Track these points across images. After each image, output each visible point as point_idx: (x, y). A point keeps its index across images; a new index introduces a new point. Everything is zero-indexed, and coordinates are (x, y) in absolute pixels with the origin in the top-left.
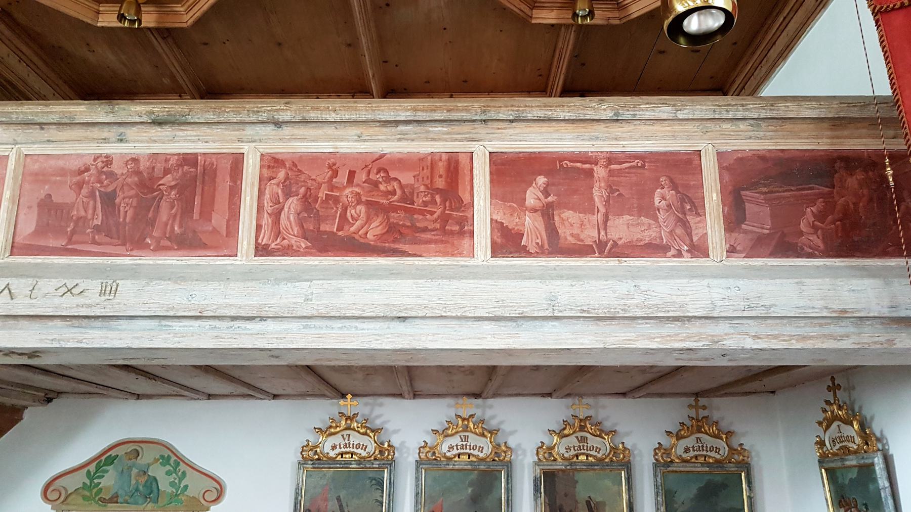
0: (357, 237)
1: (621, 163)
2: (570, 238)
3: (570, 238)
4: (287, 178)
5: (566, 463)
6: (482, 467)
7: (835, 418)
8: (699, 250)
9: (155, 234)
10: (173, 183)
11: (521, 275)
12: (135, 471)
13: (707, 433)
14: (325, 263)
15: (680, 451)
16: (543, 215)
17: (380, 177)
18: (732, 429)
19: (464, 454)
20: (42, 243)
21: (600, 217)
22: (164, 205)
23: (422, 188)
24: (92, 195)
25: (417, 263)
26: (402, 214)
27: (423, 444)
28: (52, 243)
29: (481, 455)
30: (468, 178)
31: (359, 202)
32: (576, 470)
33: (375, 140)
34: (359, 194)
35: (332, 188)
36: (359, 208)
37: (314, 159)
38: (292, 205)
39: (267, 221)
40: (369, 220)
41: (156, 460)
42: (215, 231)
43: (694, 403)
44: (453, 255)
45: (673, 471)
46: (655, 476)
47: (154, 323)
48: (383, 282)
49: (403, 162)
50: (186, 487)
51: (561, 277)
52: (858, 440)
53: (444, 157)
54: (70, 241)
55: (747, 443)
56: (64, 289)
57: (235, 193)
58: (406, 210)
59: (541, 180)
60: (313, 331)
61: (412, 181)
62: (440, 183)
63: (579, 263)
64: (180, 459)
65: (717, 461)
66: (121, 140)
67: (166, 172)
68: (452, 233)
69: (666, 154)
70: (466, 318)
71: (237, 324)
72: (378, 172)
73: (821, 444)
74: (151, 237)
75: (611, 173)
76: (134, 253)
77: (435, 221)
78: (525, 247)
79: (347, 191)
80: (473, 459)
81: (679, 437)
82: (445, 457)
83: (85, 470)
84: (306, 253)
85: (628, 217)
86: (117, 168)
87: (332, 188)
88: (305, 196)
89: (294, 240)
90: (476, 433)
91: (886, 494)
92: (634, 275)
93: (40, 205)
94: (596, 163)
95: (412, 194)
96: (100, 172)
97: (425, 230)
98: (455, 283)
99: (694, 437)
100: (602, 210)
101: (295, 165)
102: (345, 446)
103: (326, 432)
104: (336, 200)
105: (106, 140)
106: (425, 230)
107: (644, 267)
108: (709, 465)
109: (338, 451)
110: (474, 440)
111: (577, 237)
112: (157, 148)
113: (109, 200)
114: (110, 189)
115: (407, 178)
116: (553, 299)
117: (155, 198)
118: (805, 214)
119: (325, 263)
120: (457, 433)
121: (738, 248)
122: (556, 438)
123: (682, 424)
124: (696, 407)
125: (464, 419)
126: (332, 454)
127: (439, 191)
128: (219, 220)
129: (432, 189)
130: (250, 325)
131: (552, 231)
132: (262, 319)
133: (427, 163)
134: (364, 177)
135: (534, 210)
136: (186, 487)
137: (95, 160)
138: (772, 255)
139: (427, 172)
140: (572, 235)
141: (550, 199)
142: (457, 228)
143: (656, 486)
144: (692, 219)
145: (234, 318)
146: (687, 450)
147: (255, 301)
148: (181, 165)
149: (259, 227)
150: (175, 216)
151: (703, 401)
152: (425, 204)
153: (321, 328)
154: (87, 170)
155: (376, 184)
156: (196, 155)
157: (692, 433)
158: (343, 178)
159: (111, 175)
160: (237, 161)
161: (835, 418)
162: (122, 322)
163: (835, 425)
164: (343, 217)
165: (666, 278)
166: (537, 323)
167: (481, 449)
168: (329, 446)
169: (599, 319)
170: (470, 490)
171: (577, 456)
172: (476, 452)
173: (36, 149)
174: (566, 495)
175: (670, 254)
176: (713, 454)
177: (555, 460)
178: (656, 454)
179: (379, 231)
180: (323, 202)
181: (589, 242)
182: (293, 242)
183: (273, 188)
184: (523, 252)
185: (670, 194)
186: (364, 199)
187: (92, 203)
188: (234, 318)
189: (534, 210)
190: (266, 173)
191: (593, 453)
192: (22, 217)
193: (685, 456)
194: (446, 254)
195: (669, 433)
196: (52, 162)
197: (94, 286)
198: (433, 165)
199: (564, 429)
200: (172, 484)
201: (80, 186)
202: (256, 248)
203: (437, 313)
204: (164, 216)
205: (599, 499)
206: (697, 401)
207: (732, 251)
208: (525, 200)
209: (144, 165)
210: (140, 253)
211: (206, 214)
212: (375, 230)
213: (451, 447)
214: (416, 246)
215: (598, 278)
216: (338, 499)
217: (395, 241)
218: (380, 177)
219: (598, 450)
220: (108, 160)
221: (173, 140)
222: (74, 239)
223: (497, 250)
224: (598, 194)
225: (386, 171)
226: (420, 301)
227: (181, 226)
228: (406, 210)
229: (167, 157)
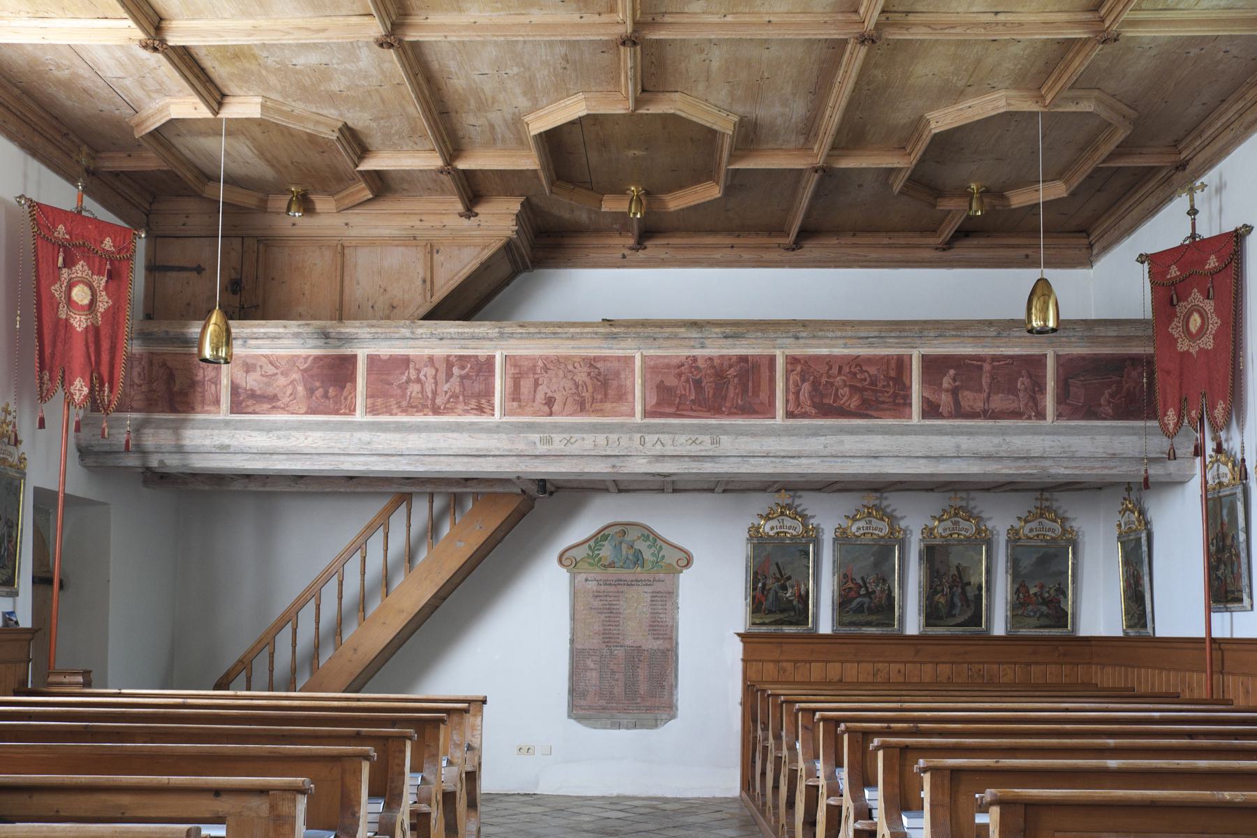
0: (844, 407)
1: (999, 361)
2: (967, 408)
3: (967, 408)
4: (802, 370)
5: (942, 539)
6: (881, 543)
7: (1127, 509)
8: (1041, 415)
9: (728, 404)
10: (735, 374)
11: (940, 432)
12: (624, 546)
13: (1047, 518)
14: (828, 423)
15: (1026, 531)
16: (952, 394)
17: (856, 370)
18: (1067, 515)
19: (868, 533)
20: (662, 410)
21: (985, 395)
22: (731, 388)
23: (882, 377)
24: (687, 381)
25: (880, 423)
26: (870, 393)
27: (837, 526)
28: (667, 410)
29: (881, 534)
30: (909, 371)
31: (845, 386)
32: (950, 545)
33: (854, 347)
34: (844, 381)
35: (829, 377)
36: (845, 389)
37: (817, 358)
38: (806, 387)
39: (791, 397)
40: (851, 397)
41: (639, 538)
42: (762, 403)
43: (1039, 497)
44: (900, 418)
45: (1020, 546)
46: (1007, 548)
47: (740, 459)
48: (866, 437)
49: (870, 360)
50: (663, 557)
51: (962, 433)
52: (1136, 523)
53: (895, 357)
54: (678, 409)
55: (1075, 525)
56: (690, 441)
57: (772, 380)
58: (872, 390)
59: (952, 372)
60: (827, 464)
61: (876, 372)
62: (893, 374)
63: (972, 423)
64: (657, 537)
65: (1053, 539)
66: (702, 347)
67: (731, 366)
68: (899, 405)
69: (1026, 355)
70: (911, 457)
71: (785, 460)
72: (856, 367)
73: (1120, 526)
74: (725, 407)
75: (994, 367)
76: (716, 416)
77: (889, 397)
78: (941, 413)
79: (838, 379)
80: (875, 537)
81: (1026, 521)
82: (854, 535)
83: (586, 545)
84: (816, 416)
85: (1001, 395)
86: (700, 364)
87: (829, 377)
88: (813, 382)
89: (808, 409)
90: (877, 518)
91: (1145, 556)
92: (1004, 432)
93: (657, 387)
94: (985, 361)
95: (876, 380)
96: (691, 367)
97: (883, 402)
98: (906, 438)
99: (1037, 521)
100: (987, 391)
101: (806, 362)
102: (781, 527)
103: (768, 518)
104: (832, 384)
105: (693, 347)
106: (883, 402)
107: (1008, 426)
108: (1047, 541)
109: (775, 531)
110: (876, 523)
111: (971, 407)
112: (725, 352)
113: (698, 384)
114: (698, 377)
115: (873, 370)
116: (958, 447)
117: (725, 383)
118: (1104, 393)
119: (828, 423)
120: (864, 518)
121: (1064, 414)
122: (936, 523)
123: (1030, 512)
124: (1041, 499)
125: (869, 508)
126: (772, 533)
127: (892, 378)
128: (764, 396)
129: (890, 379)
130: (792, 461)
131: (957, 403)
132: (799, 457)
133: (885, 360)
134: (848, 370)
135: (947, 391)
136: (663, 557)
137: (687, 359)
138: (1082, 419)
139: (884, 367)
140: (969, 406)
141: (957, 384)
142: (902, 401)
143: (1007, 556)
144: (1038, 396)
145: (784, 457)
146: (1031, 530)
147: (796, 448)
148: (738, 363)
149: (787, 401)
150: (738, 394)
151: (1046, 495)
152: (884, 386)
153: (831, 462)
154: (683, 365)
155: (855, 374)
156: (747, 356)
157: (1036, 518)
158: (835, 371)
159: (697, 368)
160: (772, 359)
161: (1127, 509)
162: (721, 458)
163: (1128, 512)
164: (836, 395)
165: (1020, 434)
166: (949, 459)
167: (881, 530)
168: (767, 528)
169: (983, 457)
170: (872, 559)
171: (951, 535)
172: (877, 532)
173: (652, 352)
174: (942, 562)
175: (1024, 417)
176: (1050, 533)
177: (935, 537)
178: (1009, 533)
179: (857, 403)
180: (824, 385)
181: (978, 410)
182: (808, 410)
183: (794, 377)
184: (939, 416)
185: (1027, 381)
186: (848, 383)
187: (688, 386)
188: (784, 457)
189: (947, 391)
190: (790, 367)
191: (963, 532)
192: (648, 394)
193: (1029, 535)
194: (895, 417)
195: (1019, 519)
196: (662, 360)
197: (707, 439)
198: (888, 362)
199: (943, 515)
200: (653, 554)
201: (680, 375)
202: (786, 413)
203: (896, 454)
204: (731, 394)
205: (965, 565)
206: (1041, 494)
207: (1059, 416)
208: (941, 384)
209: (716, 362)
210: (719, 416)
211: (756, 393)
212: (854, 403)
213: (859, 529)
214: (879, 413)
215: (983, 434)
216: (777, 564)
217: (867, 409)
218: (856, 370)
219: (967, 530)
220: (695, 359)
221: (734, 346)
222: (680, 407)
223: (925, 415)
224: (985, 381)
225: (860, 366)
226: (887, 448)
227: (742, 400)
228: (872, 390)
229: (730, 358)
